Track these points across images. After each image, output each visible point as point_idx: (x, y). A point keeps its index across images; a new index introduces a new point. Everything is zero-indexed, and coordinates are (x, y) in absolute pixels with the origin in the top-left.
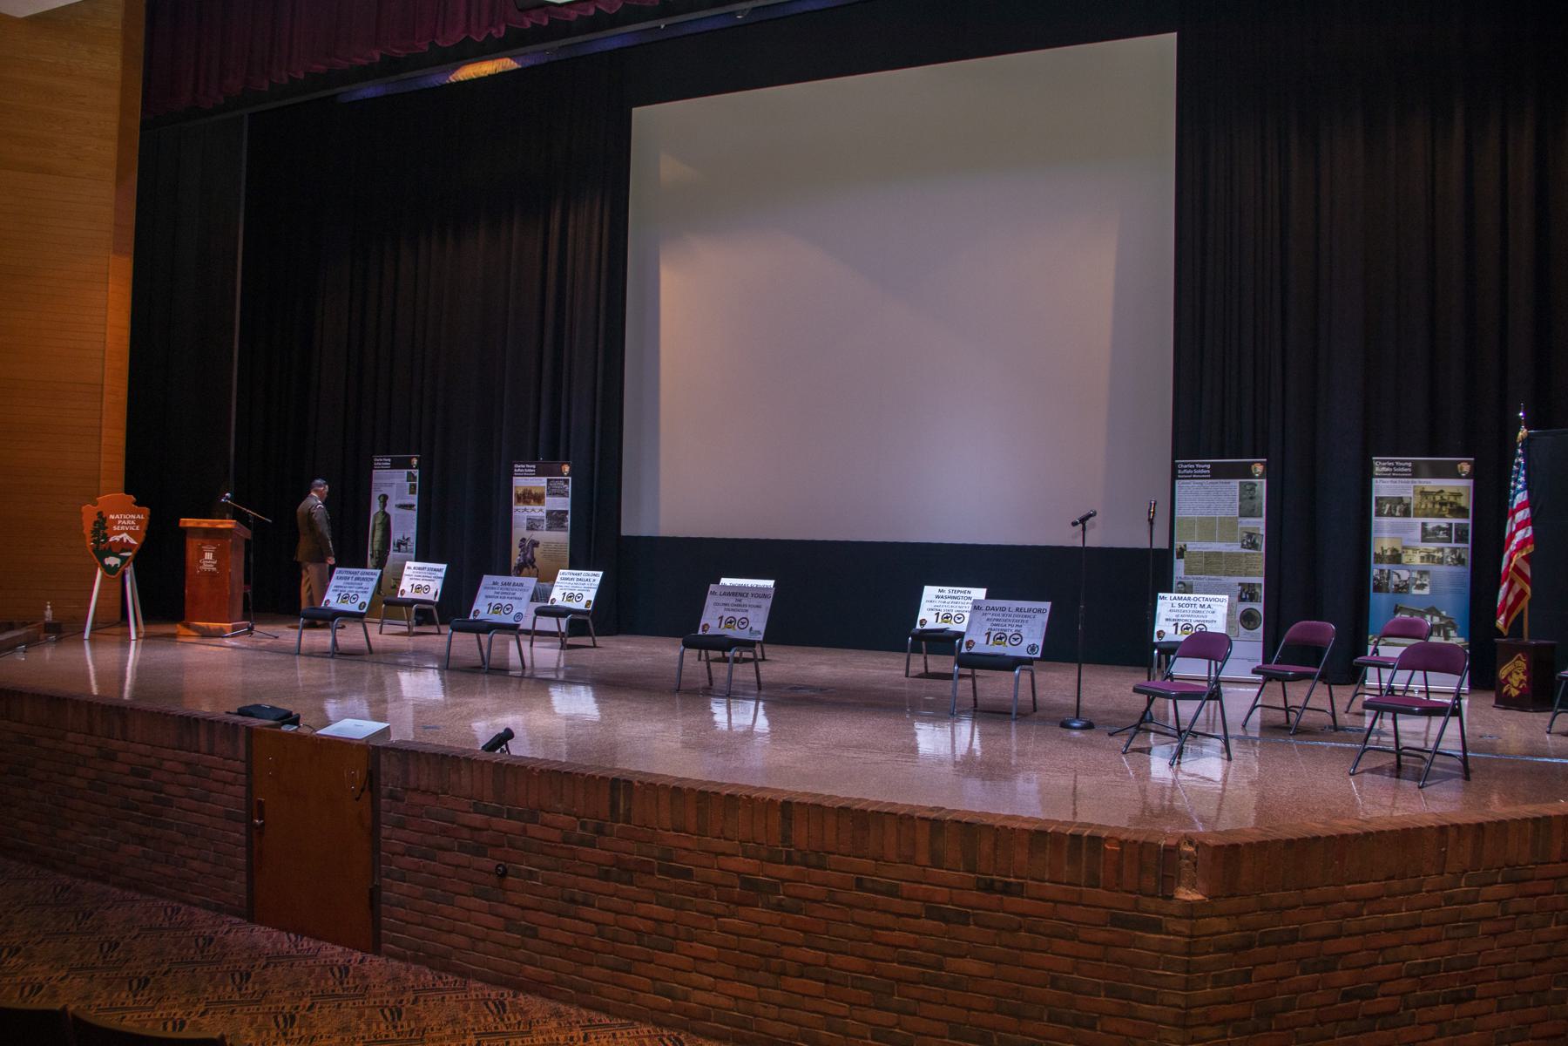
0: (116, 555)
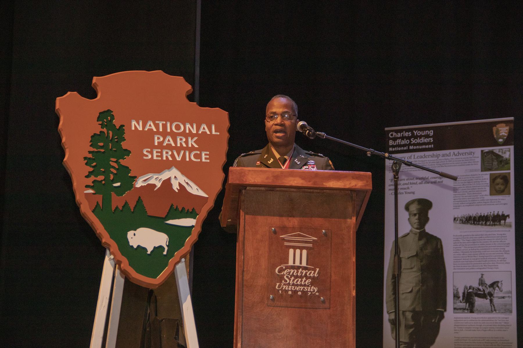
0: (157, 224)
